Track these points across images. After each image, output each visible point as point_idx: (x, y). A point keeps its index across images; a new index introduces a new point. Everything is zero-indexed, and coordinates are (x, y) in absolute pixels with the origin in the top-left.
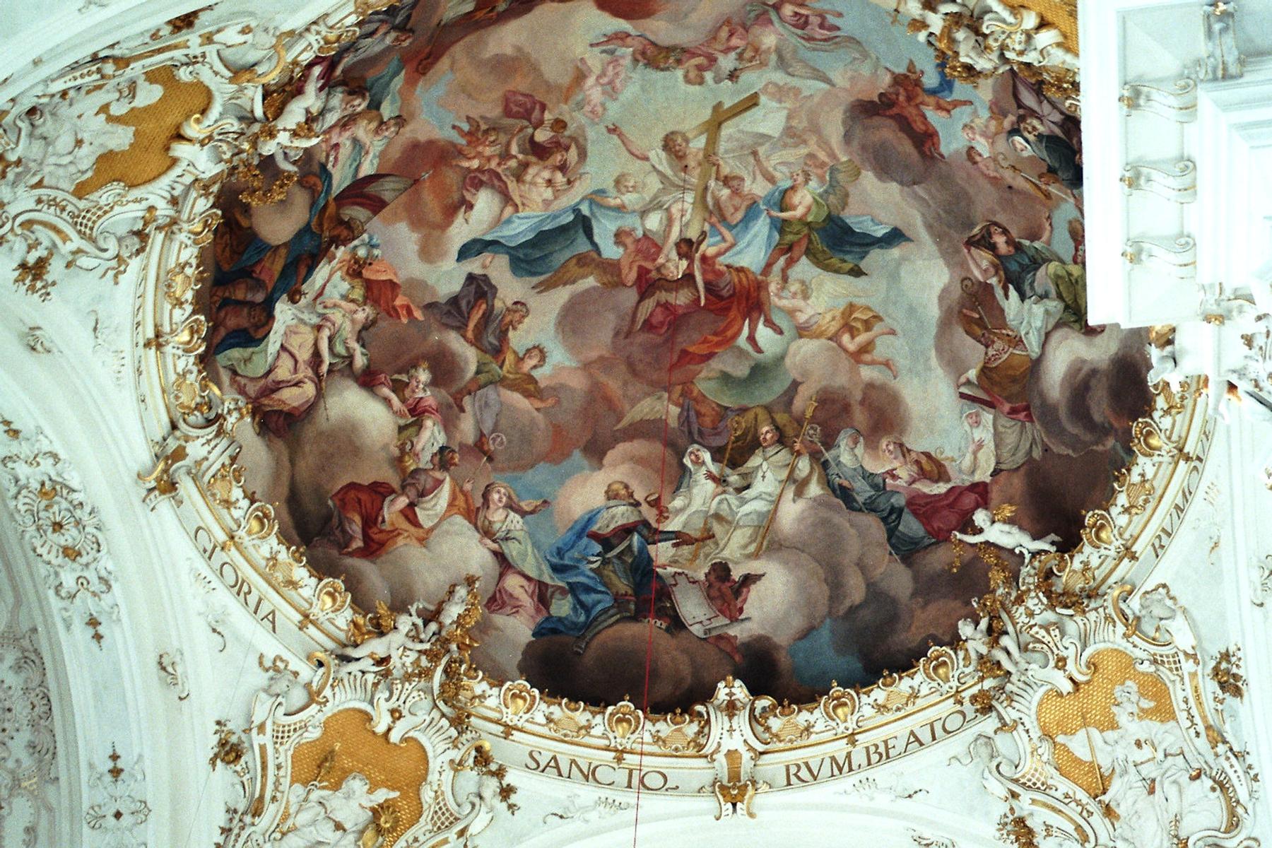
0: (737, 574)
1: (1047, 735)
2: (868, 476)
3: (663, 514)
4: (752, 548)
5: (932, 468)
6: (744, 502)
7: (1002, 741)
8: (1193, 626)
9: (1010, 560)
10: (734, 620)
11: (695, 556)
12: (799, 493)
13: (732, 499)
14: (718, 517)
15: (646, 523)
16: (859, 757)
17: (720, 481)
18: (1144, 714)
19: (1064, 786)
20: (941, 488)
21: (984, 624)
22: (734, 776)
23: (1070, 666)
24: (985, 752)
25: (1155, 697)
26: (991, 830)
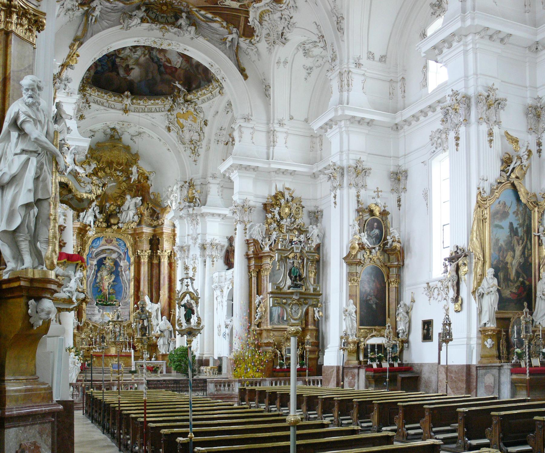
0: (130, 67)
1: (177, 117)
2: (158, 58)
3: (120, 53)
4: (134, 63)
5: (169, 61)
6: (134, 55)
7: (170, 116)
8: (204, 115)
9: (179, 90)
10: (128, 75)
11: (123, 62)
12: (144, 56)
13: (132, 54)
14: (129, 56)
15: (116, 54)
16: (146, 110)
17: (131, 50)
18: (192, 121)
19: (177, 125)
20: (170, 65)
21: (172, 98)
22: (126, 108)
23: (184, 111)
24: (166, 116)
25: (195, 119)
26: (164, 127)
